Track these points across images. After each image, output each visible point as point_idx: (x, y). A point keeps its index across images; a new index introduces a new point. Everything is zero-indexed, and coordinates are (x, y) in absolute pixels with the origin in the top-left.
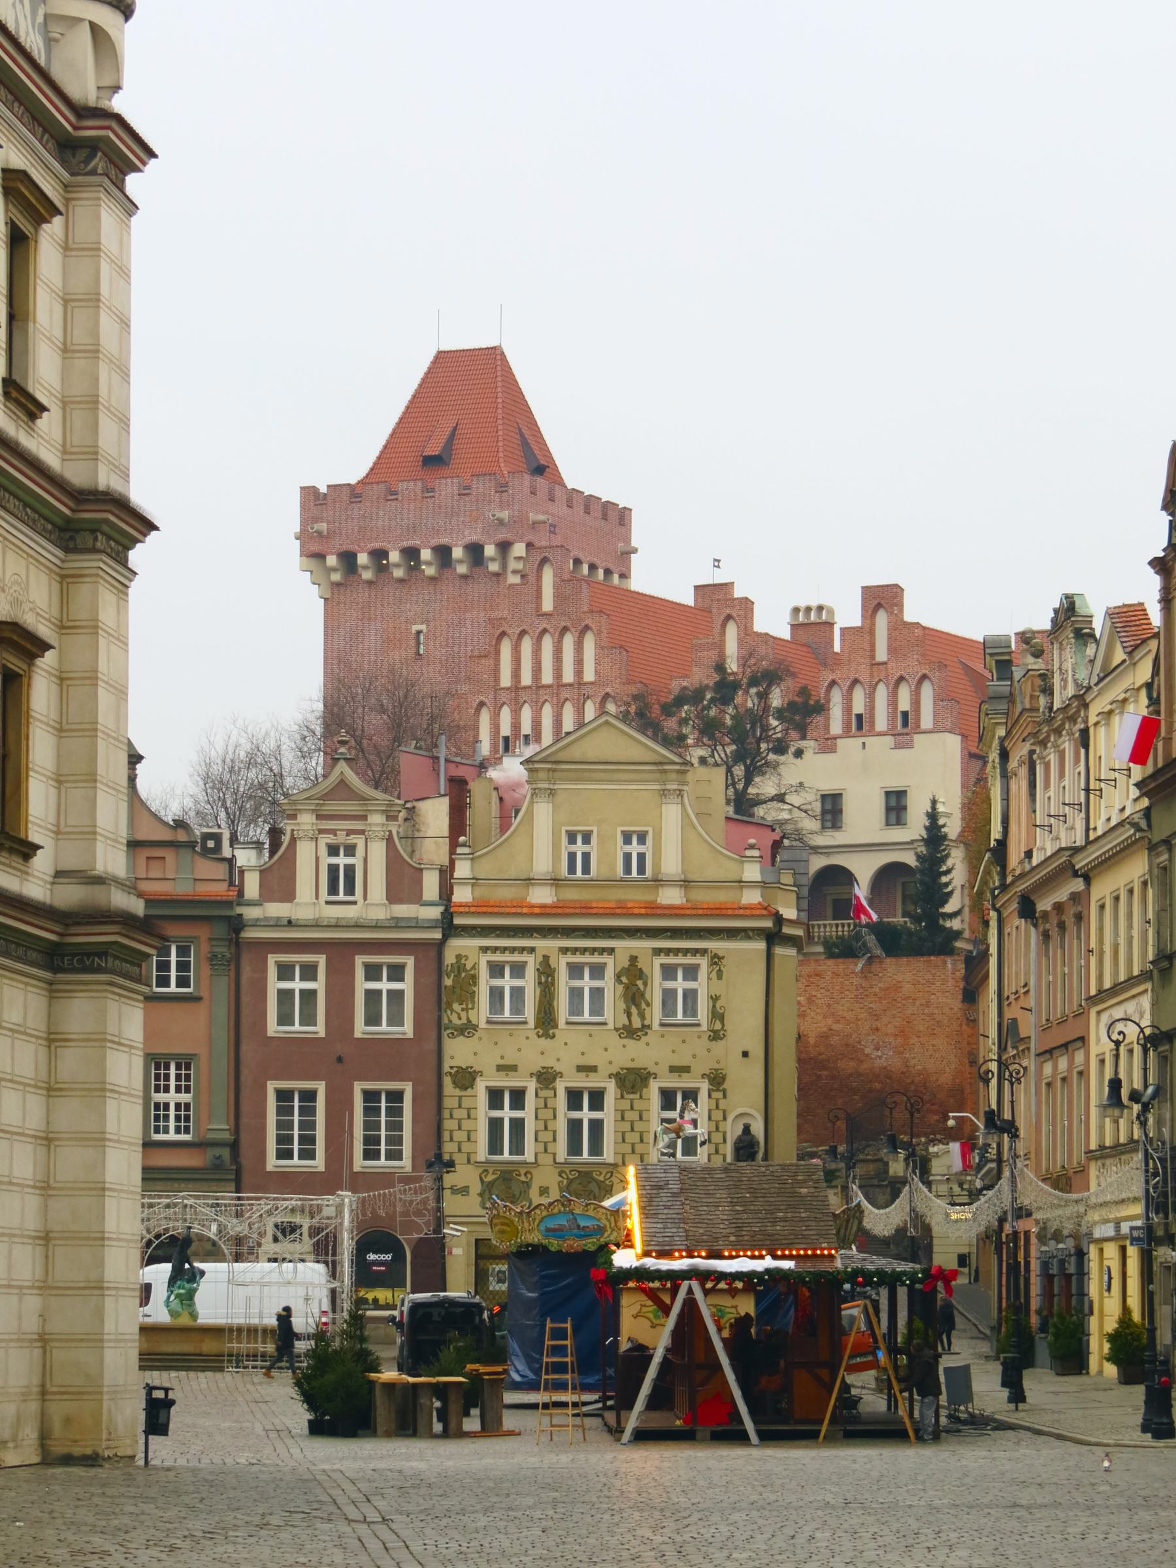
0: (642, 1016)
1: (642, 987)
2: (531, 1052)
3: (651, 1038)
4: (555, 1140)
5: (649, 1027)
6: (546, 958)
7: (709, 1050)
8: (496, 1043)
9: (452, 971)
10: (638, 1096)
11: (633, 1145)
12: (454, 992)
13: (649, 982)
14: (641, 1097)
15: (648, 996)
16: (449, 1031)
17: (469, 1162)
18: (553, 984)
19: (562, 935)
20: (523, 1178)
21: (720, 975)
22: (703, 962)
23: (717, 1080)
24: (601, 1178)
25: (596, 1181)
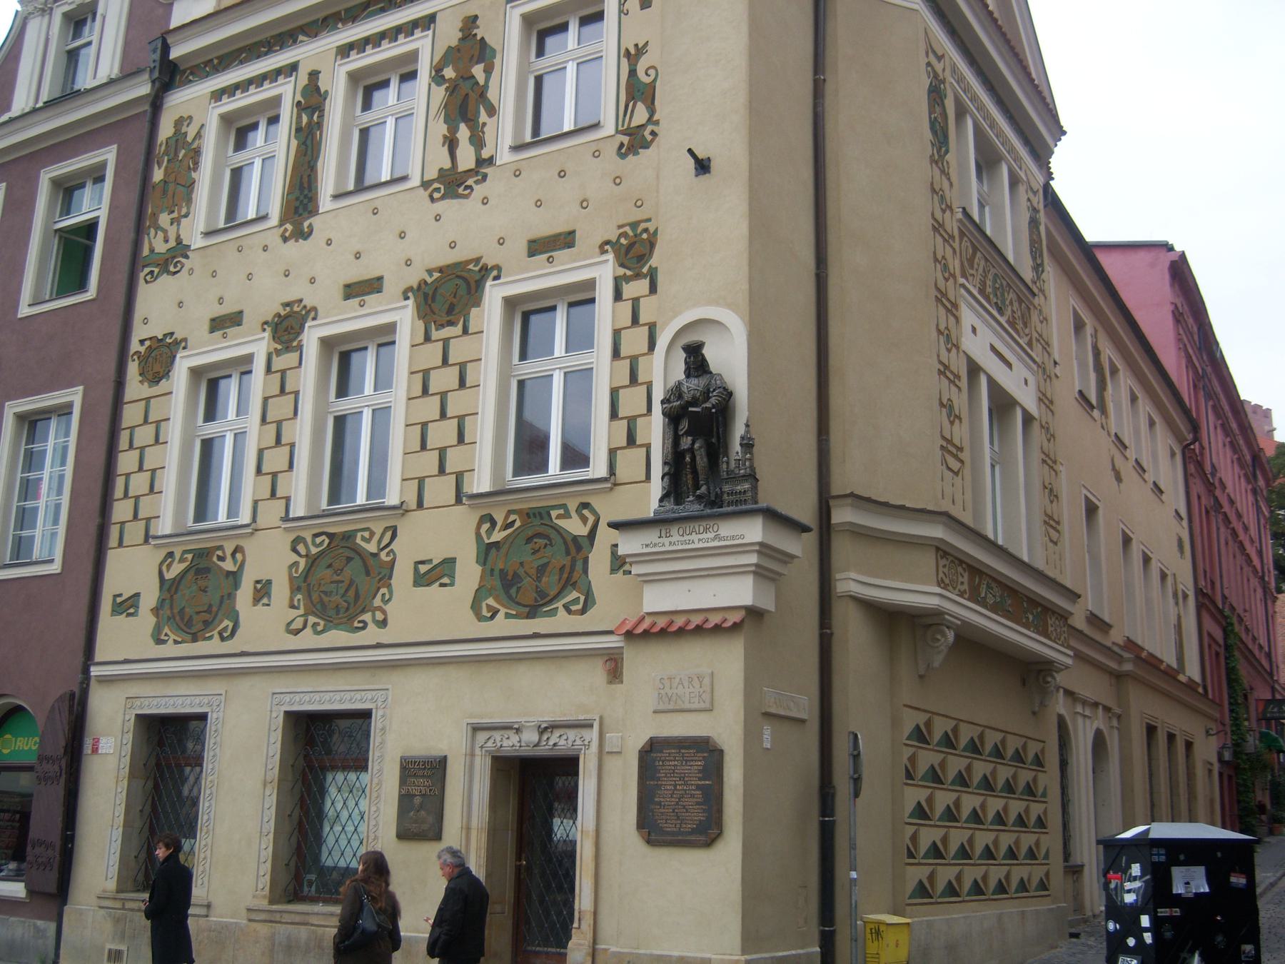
0: (478, 141)
1: (482, 82)
2: (265, 273)
3: (495, 185)
5: (490, 161)
6: (314, 75)
7: (617, 181)
8: (214, 274)
9: (166, 153)
10: (458, 329)
11: (442, 452)
12: (165, 192)
13: (497, 61)
14: (465, 331)
15: (492, 95)
16: (147, 270)
17: (147, 538)
18: (319, 125)
19: (345, 22)
20: (228, 565)
23: (635, 251)
24: (372, 547)
25: (358, 552)
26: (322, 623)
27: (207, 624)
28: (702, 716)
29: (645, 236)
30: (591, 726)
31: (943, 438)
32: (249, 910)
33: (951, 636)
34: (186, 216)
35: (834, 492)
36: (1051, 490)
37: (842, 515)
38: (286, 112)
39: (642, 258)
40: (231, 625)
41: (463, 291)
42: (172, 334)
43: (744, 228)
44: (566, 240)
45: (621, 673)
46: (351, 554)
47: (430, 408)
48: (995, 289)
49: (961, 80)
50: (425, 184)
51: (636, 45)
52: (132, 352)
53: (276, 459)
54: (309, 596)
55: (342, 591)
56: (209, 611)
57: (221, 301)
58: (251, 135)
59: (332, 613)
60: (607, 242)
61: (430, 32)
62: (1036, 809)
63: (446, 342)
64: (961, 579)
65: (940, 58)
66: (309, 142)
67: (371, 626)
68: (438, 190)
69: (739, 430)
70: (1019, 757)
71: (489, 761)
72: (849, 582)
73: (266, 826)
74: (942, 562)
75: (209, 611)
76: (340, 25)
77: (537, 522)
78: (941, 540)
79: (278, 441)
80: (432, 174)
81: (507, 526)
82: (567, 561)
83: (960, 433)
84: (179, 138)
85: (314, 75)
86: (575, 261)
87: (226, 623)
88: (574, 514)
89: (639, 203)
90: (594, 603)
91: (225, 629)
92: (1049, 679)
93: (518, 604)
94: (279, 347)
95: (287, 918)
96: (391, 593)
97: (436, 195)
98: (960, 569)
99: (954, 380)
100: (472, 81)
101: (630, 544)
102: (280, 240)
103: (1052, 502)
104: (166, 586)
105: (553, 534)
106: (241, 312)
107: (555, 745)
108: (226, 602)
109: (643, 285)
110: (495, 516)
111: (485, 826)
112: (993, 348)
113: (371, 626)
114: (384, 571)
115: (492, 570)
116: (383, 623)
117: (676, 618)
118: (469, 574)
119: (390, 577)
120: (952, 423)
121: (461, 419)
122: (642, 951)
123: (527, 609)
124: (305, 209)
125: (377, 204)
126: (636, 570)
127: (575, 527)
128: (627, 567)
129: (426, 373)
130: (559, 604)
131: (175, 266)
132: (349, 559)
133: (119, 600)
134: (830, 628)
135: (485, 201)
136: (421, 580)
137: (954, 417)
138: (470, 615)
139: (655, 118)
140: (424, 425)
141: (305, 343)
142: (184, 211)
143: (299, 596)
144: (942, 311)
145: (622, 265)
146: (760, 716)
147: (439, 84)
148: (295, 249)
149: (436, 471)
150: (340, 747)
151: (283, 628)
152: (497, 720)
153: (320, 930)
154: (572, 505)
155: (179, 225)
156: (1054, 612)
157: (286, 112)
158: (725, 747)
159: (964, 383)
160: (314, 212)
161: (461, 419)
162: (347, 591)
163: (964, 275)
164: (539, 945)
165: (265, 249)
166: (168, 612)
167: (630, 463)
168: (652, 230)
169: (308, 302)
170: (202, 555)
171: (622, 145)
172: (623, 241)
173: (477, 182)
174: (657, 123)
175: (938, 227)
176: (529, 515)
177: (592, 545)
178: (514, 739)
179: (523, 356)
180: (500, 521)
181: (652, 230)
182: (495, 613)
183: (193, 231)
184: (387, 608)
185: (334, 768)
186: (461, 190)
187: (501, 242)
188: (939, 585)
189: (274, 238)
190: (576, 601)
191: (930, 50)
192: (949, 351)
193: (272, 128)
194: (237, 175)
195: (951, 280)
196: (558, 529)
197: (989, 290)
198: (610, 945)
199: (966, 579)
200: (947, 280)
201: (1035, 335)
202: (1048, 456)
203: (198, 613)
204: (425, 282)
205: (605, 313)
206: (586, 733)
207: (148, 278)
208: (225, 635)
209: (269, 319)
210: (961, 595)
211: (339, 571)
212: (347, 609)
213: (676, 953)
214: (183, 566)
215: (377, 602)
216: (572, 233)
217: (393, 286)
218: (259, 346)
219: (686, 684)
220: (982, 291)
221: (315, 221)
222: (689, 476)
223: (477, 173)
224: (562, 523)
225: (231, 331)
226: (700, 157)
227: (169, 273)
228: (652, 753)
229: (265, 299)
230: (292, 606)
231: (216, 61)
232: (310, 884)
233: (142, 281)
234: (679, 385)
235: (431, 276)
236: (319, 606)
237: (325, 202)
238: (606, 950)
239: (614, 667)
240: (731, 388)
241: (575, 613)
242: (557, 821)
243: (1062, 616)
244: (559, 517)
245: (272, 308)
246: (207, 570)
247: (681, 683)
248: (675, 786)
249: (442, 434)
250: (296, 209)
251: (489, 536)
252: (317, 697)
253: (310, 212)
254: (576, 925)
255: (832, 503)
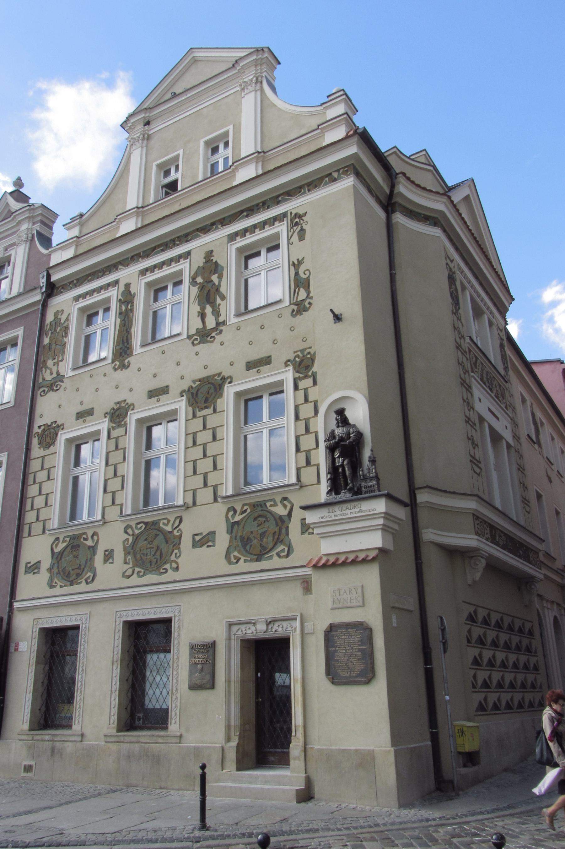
0: (216, 313)
1: (217, 283)
3: (227, 334)
4: (123, 487)
5: (224, 323)
6: (128, 286)
7: (292, 329)
8: (77, 390)
9: (50, 329)
10: (211, 410)
11: (205, 475)
12: (50, 349)
14: (215, 411)
15: (223, 289)
16: (41, 390)
18: (132, 310)
19: (143, 257)
20: (90, 543)
21: (302, 237)
22: (282, 228)
23: (304, 364)
24: (169, 528)
26: (143, 571)
27: (78, 575)
28: (359, 610)
29: (309, 356)
30: (295, 619)
31: (471, 456)
32: (105, 736)
33: (484, 562)
34: (62, 361)
35: (417, 486)
36: (524, 485)
37: (422, 497)
38: (114, 305)
39: (308, 368)
40: (92, 575)
41: (212, 390)
42: (56, 422)
43: (362, 348)
44: (267, 361)
45: (311, 589)
46: (158, 533)
47: (197, 452)
48: (488, 379)
49: (462, 272)
50: (189, 337)
51: (298, 260)
52: (34, 433)
53: (114, 485)
54: (135, 556)
55: (153, 553)
56: (79, 568)
57: (82, 403)
58: (94, 319)
59: (148, 565)
60: (289, 361)
61: (188, 260)
62: (533, 660)
63: (204, 417)
64: (486, 531)
65: (452, 261)
66: (126, 319)
67: (170, 571)
68: (196, 339)
69: (367, 453)
70: (521, 631)
71: (239, 642)
72: (429, 535)
73: (114, 687)
74: (477, 522)
75: (79, 568)
76: (140, 260)
77: (259, 509)
78: (476, 510)
79: (115, 475)
80: (193, 331)
81: (243, 512)
82: (277, 529)
83: (478, 453)
84: (57, 321)
85: (128, 286)
86: (272, 371)
87: (89, 574)
88: (279, 504)
89: (304, 340)
90: (293, 551)
91: (89, 577)
92: (533, 587)
93: (251, 554)
94: (114, 425)
95: (127, 739)
96: (180, 552)
97: (196, 342)
98: (485, 526)
99: (473, 425)
100: (212, 283)
101: (312, 517)
102: (112, 371)
103: (524, 491)
104: (55, 557)
105: (269, 515)
106: (93, 408)
107: (276, 631)
108: (89, 563)
109: (309, 381)
110: (236, 508)
111: (239, 679)
112: (490, 410)
113: (170, 571)
114: (176, 541)
115: (236, 537)
116: (177, 569)
117: (339, 556)
118: (223, 540)
119: (179, 544)
120: (474, 448)
121: (215, 457)
122: (334, 747)
123: (256, 557)
124: (126, 353)
125: (164, 348)
126: (316, 531)
127: (280, 511)
128: (310, 530)
129: (194, 434)
130: (274, 553)
131: (57, 387)
132: (156, 535)
133: (29, 565)
134: (421, 560)
135: (222, 344)
136: (197, 544)
137: (475, 446)
138: (224, 561)
139: (311, 295)
140: (195, 462)
141: (128, 422)
142: (60, 358)
143: (130, 557)
144: (464, 390)
145: (297, 372)
146: (389, 609)
147: (194, 286)
148: (121, 374)
149: (202, 486)
150: (154, 639)
151: (121, 575)
152: (242, 619)
153: (147, 745)
154: (278, 499)
155: (58, 365)
156: (532, 550)
157: (114, 305)
158: (373, 627)
159: (477, 427)
160: (131, 354)
161: (215, 457)
162: (156, 553)
163: (473, 372)
164: (271, 748)
165: (105, 375)
166: (57, 570)
167: (308, 475)
168: (312, 353)
169: (129, 401)
170: (75, 538)
171: (293, 311)
172: (297, 359)
173: (216, 334)
174: (312, 298)
175: (458, 347)
176: (254, 506)
177: (290, 520)
178: (253, 629)
179: (246, 423)
180: (238, 509)
181: (312, 353)
182: (238, 560)
183: (66, 367)
184: (179, 560)
185: (151, 651)
186: (209, 339)
187: (232, 364)
188: (476, 535)
189: (109, 369)
190: (283, 550)
191: (447, 257)
192: (469, 410)
193: (107, 314)
194: (88, 338)
195: (467, 374)
196: (271, 513)
197: (485, 379)
198: (316, 745)
199: (488, 532)
200: (465, 374)
201: (508, 403)
202: (520, 466)
203: (73, 570)
204: (192, 387)
205: (289, 397)
206: (293, 623)
207: (42, 394)
208: (89, 581)
209: (108, 411)
210: (487, 539)
211: (151, 542)
212: (157, 562)
213: (353, 748)
214: (64, 545)
215: (173, 557)
216: (269, 357)
217: (175, 390)
218: (103, 426)
219: (348, 592)
220: (482, 380)
221: (132, 359)
222: (342, 479)
223: (217, 330)
224: (273, 509)
225: (88, 418)
226: (337, 313)
227: (53, 390)
228: (331, 632)
229: (106, 400)
230: (126, 563)
231: (75, 282)
232: (139, 718)
233: (39, 396)
234: (333, 432)
235: (195, 383)
236: (140, 562)
237: (137, 349)
238: (312, 748)
239: (307, 586)
240: (361, 431)
241: (283, 557)
242: (277, 675)
243: (536, 552)
244: (271, 506)
245: (109, 405)
246: (78, 546)
247: (345, 592)
248: (346, 650)
249: (205, 465)
250: (121, 355)
251: (233, 518)
252: (141, 612)
253: (128, 355)
254: (293, 734)
255: (417, 492)
